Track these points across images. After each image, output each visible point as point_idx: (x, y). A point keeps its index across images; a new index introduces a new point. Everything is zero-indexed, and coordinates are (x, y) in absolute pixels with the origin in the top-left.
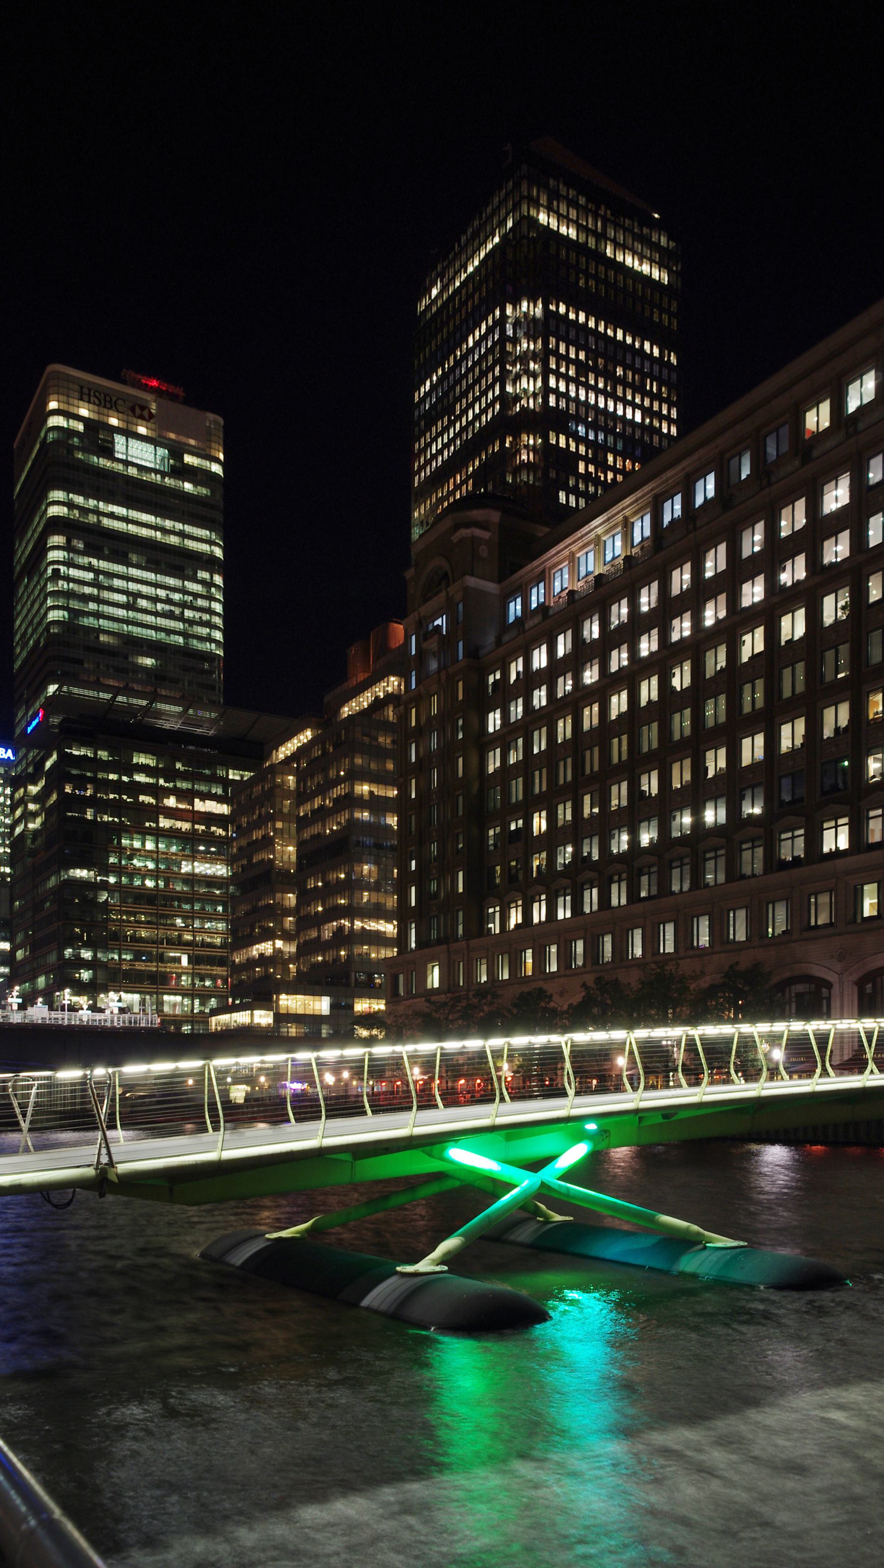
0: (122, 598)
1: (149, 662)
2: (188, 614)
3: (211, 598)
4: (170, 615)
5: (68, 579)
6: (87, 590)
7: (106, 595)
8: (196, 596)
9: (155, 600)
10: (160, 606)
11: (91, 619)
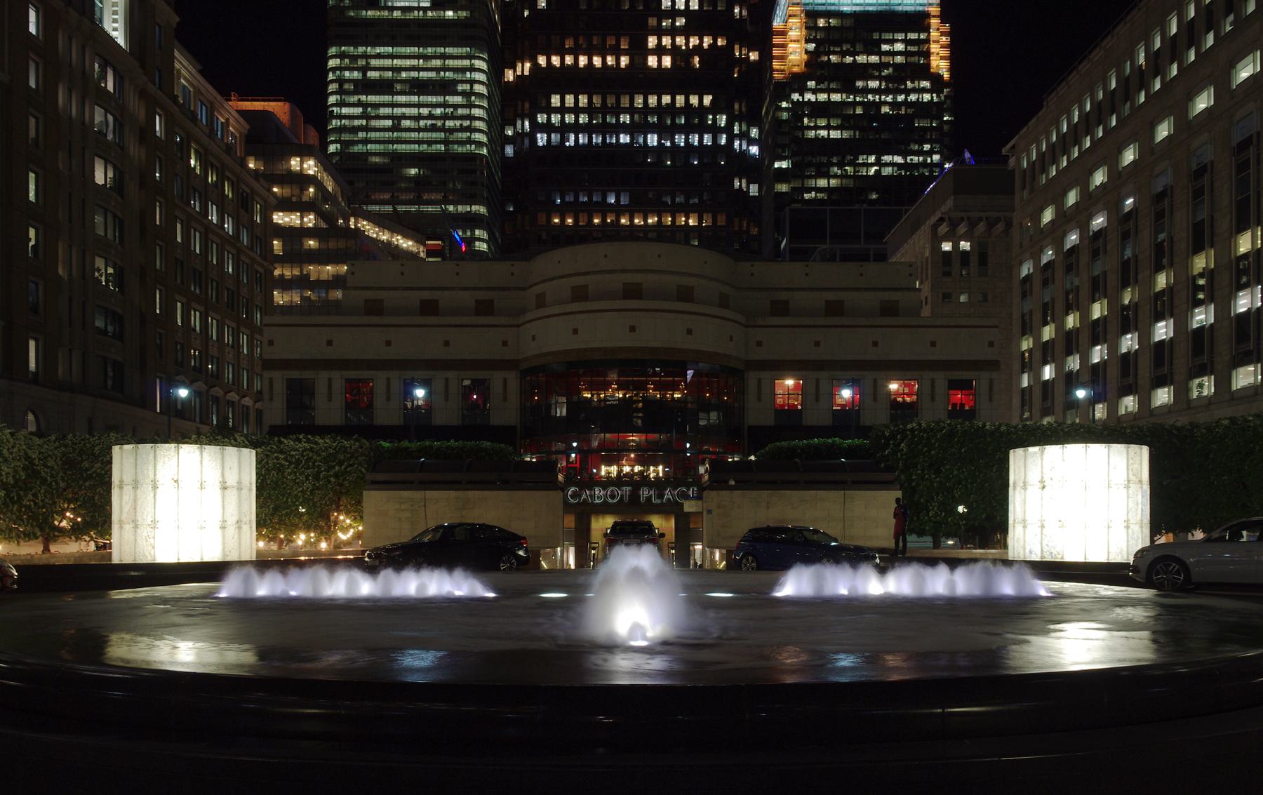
0: (389, 123)
1: (413, 171)
2: (450, 123)
3: (471, 106)
4: (433, 128)
5: (340, 117)
6: (356, 123)
7: (374, 123)
8: (456, 106)
9: (418, 118)
10: (422, 123)
11: (360, 146)
